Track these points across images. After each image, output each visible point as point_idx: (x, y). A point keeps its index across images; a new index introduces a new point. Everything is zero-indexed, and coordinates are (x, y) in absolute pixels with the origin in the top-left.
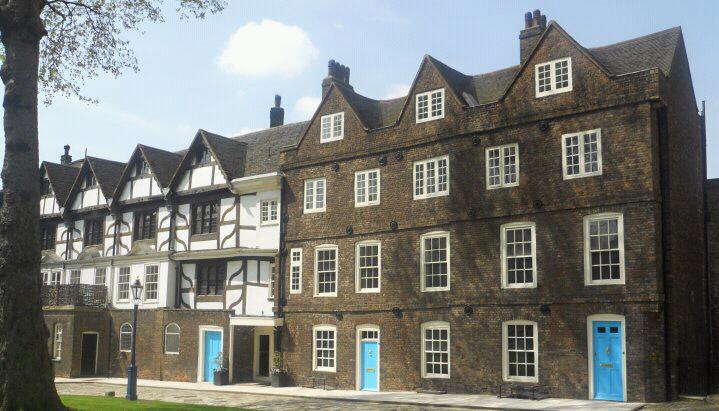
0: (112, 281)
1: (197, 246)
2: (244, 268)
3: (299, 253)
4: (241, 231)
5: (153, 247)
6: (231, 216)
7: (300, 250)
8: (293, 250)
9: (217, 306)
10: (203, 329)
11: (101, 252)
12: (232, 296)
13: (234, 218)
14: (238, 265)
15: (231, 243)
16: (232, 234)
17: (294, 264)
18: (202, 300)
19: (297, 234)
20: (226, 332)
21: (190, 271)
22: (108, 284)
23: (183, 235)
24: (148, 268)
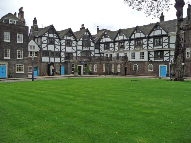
0: (129, 56)
1: (155, 48)
2: (170, 52)
3: (189, 49)
4: (170, 44)
5: (142, 48)
6: (167, 41)
7: (190, 48)
8: (187, 48)
9: (162, 60)
10: (160, 65)
11: (124, 49)
12: (165, 59)
13: (168, 41)
14: (168, 51)
15: (167, 47)
16: (167, 45)
17: (187, 51)
18: (155, 59)
19: (189, 45)
20: (168, 66)
21: (152, 53)
22: (128, 56)
23: (152, 45)
24: (141, 53)
